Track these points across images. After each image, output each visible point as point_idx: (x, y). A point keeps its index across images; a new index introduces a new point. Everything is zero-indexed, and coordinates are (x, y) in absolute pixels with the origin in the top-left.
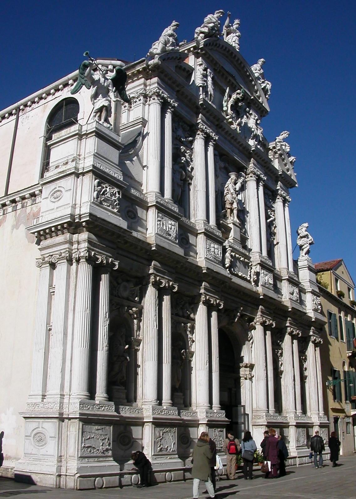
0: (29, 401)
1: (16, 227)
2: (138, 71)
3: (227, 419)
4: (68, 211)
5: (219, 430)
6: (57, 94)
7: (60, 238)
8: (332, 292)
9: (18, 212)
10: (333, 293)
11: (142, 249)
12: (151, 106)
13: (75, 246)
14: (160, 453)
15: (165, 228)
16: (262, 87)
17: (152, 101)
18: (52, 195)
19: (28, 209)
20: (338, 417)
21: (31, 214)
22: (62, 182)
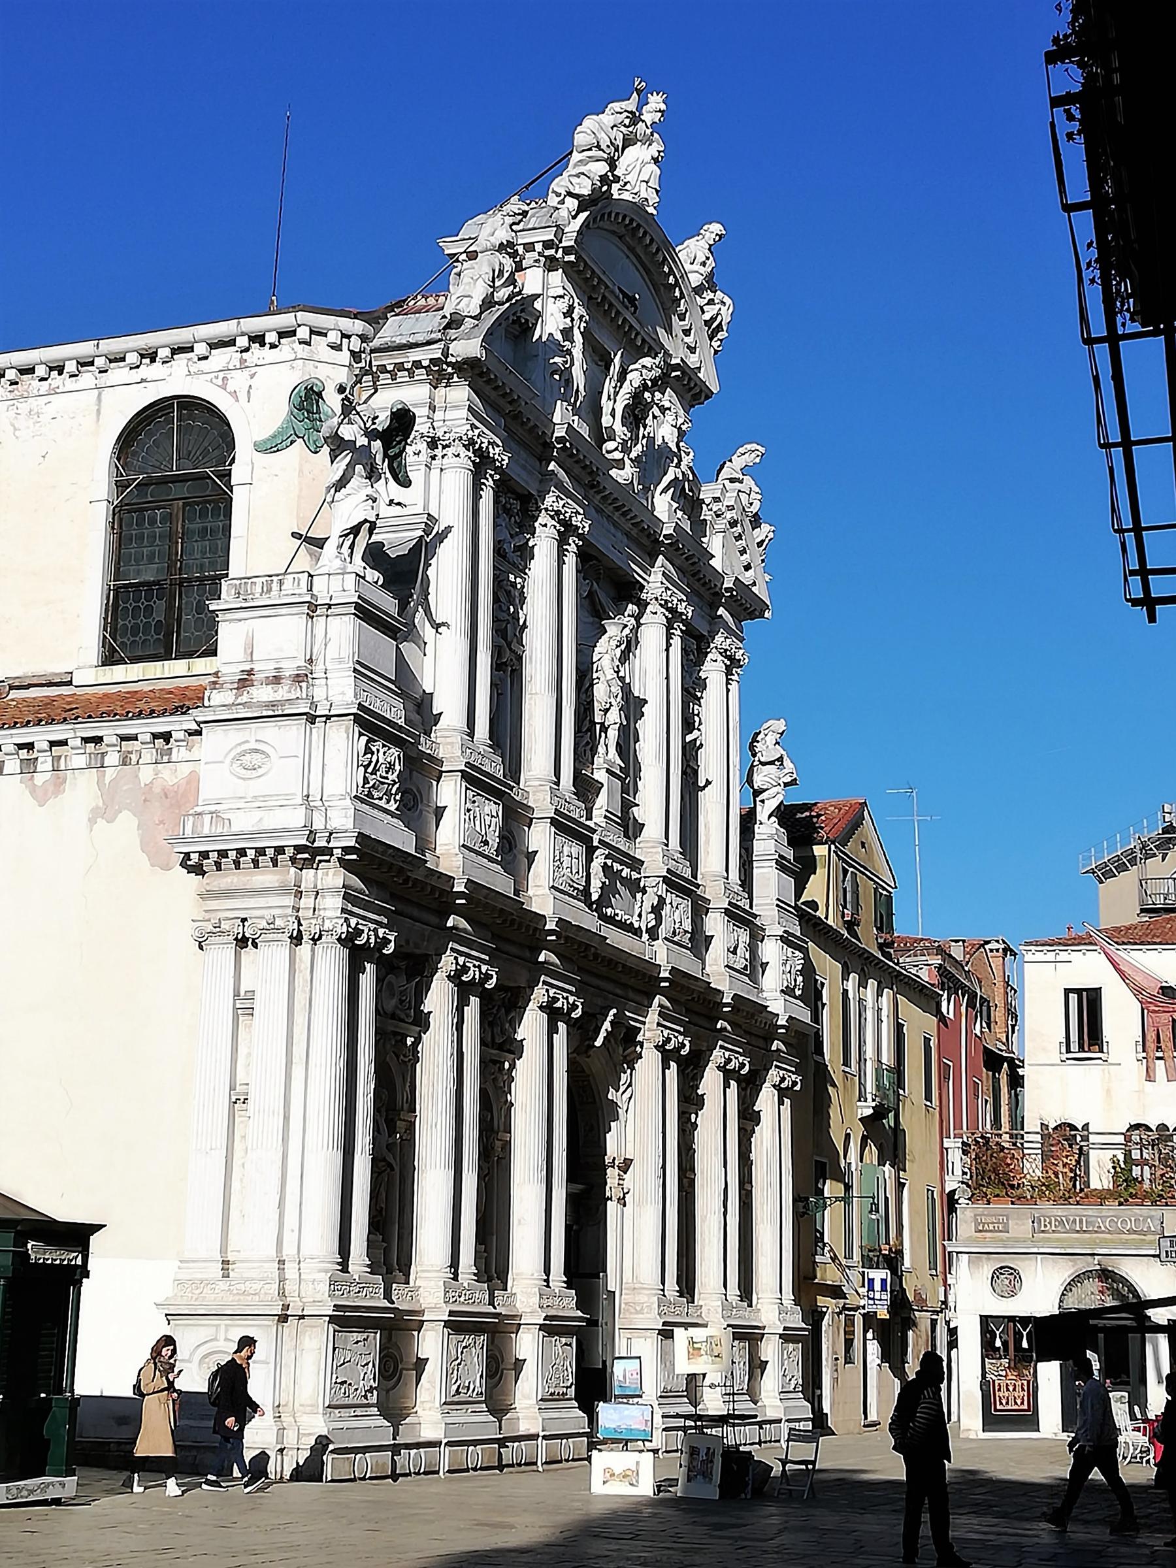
0: (183, 1276)
1: (104, 812)
2: (417, 364)
3: (580, 1314)
4: (296, 818)
5: (564, 1340)
6: (149, 371)
7: (266, 877)
8: (826, 918)
9: (110, 773)
10: (830, 922)
11: (432, 892)
12: (447, 475)
13: (307, 902)
14: (456, 1399)
15: (478, 829)
16: (707, 317)
17: (450, 461)
18: (237, 758)
19: (146, 774)
20: (824, 1310)
21: (157, 789)
22: (269, 732)
